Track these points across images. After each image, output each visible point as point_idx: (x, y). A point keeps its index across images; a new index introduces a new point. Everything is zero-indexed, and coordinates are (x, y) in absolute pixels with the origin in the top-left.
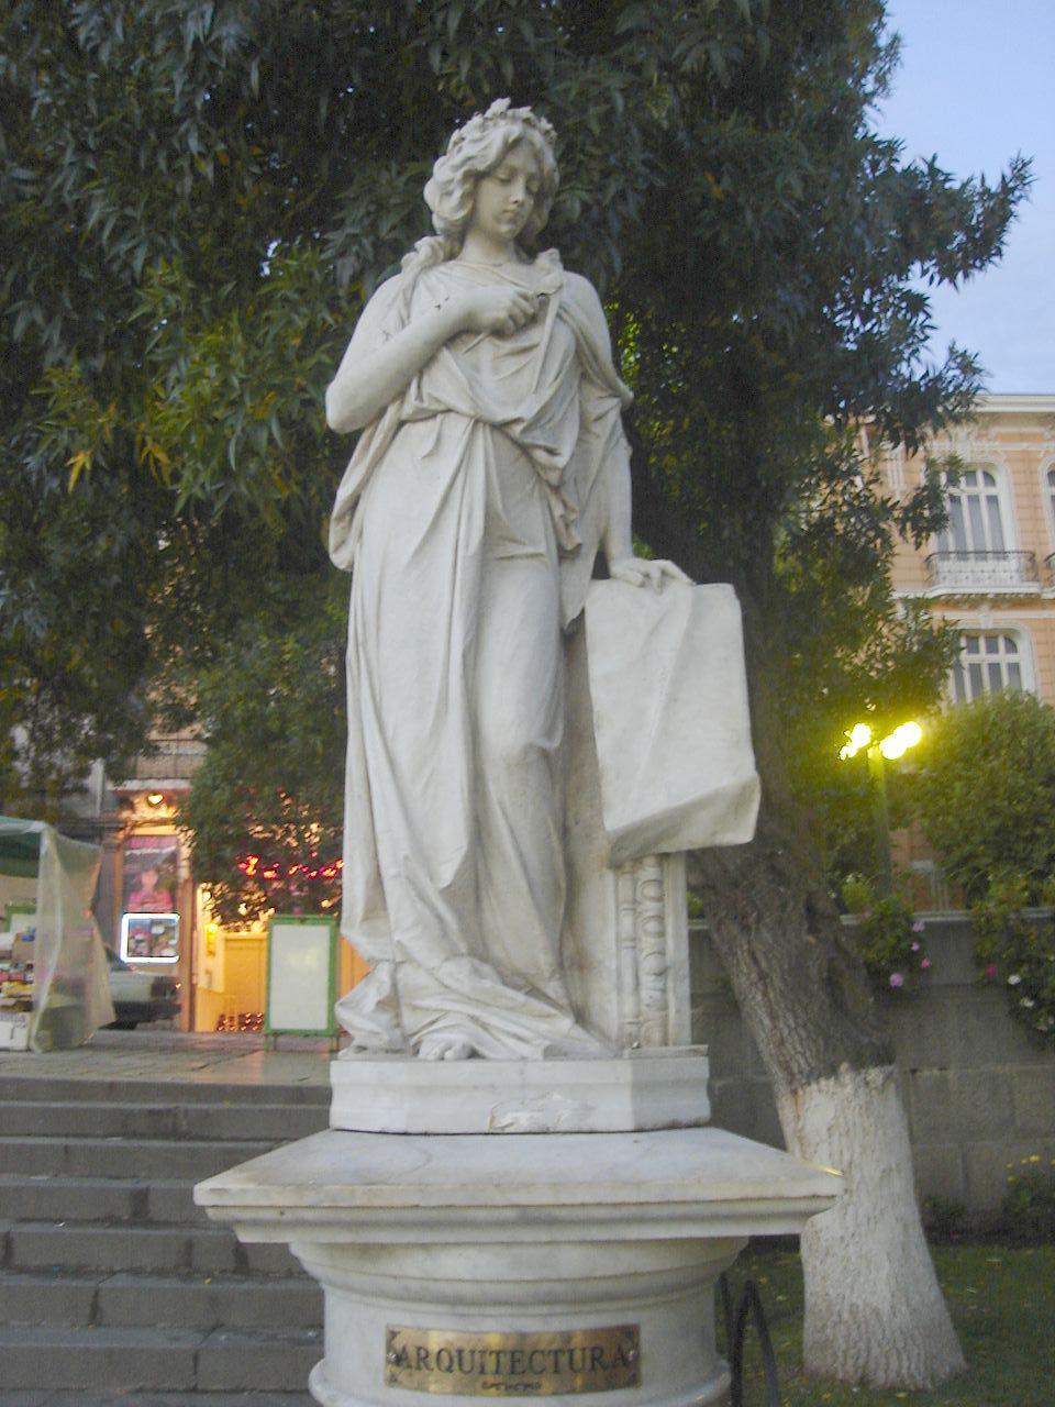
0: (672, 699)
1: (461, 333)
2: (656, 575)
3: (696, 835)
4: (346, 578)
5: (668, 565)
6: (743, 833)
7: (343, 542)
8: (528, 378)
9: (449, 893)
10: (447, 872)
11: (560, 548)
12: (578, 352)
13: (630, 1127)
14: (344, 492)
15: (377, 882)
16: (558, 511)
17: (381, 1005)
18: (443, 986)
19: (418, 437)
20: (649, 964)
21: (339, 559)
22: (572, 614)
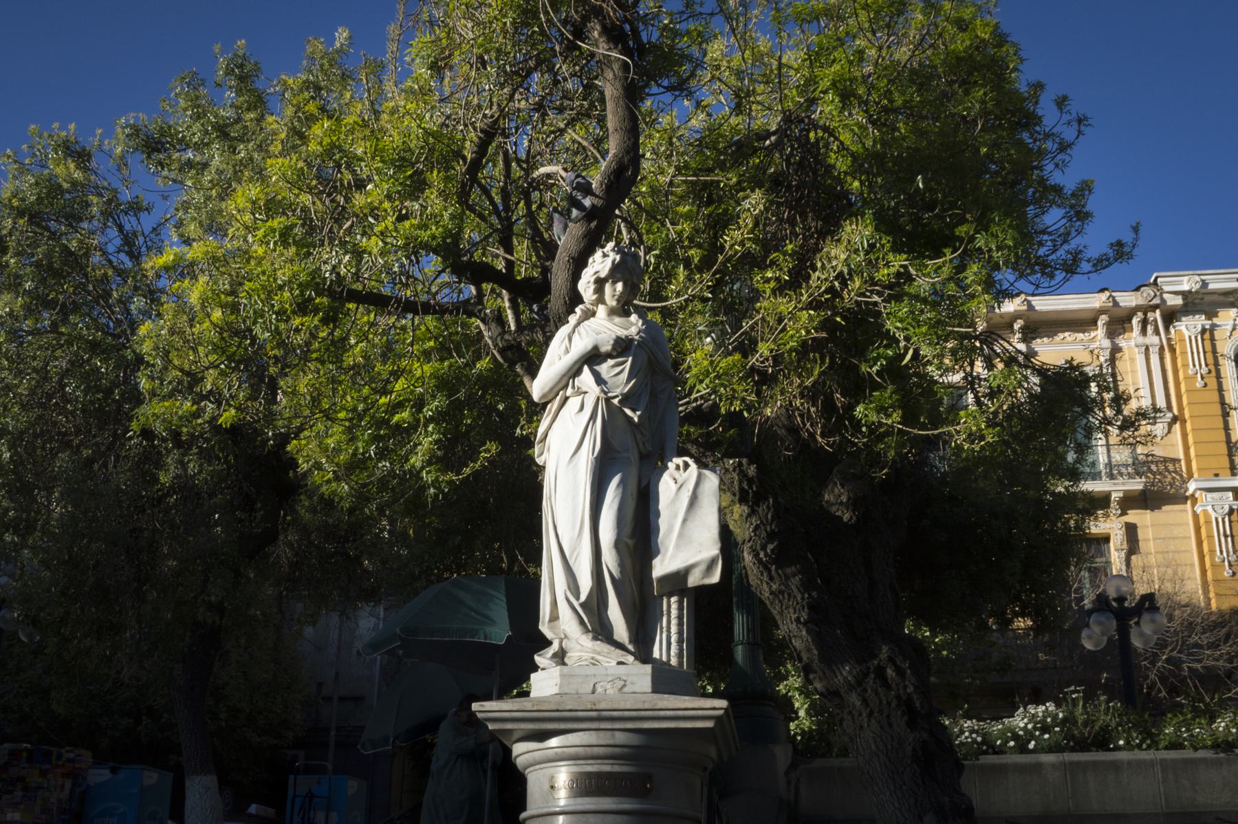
0: (685, 520)
1: (593, 358)
2: (681, 465)
3: (693, 580)
4: (542, 468)
5: (687, 459)
6: (715, 578)
7: (542, 454)
8: (625, 375)
9: (582, 605)
10: (583, 598)
11: (640, 453)
12: (649, 359)
13: (650, 690)
14: (541, 430)
15: (554, 603)
16: (639, 437)
17: (555, 655)
18: (581, 645)
19: (574, 403)
20: (674, 638)
21: (540, 461)
22: (644, 483)
